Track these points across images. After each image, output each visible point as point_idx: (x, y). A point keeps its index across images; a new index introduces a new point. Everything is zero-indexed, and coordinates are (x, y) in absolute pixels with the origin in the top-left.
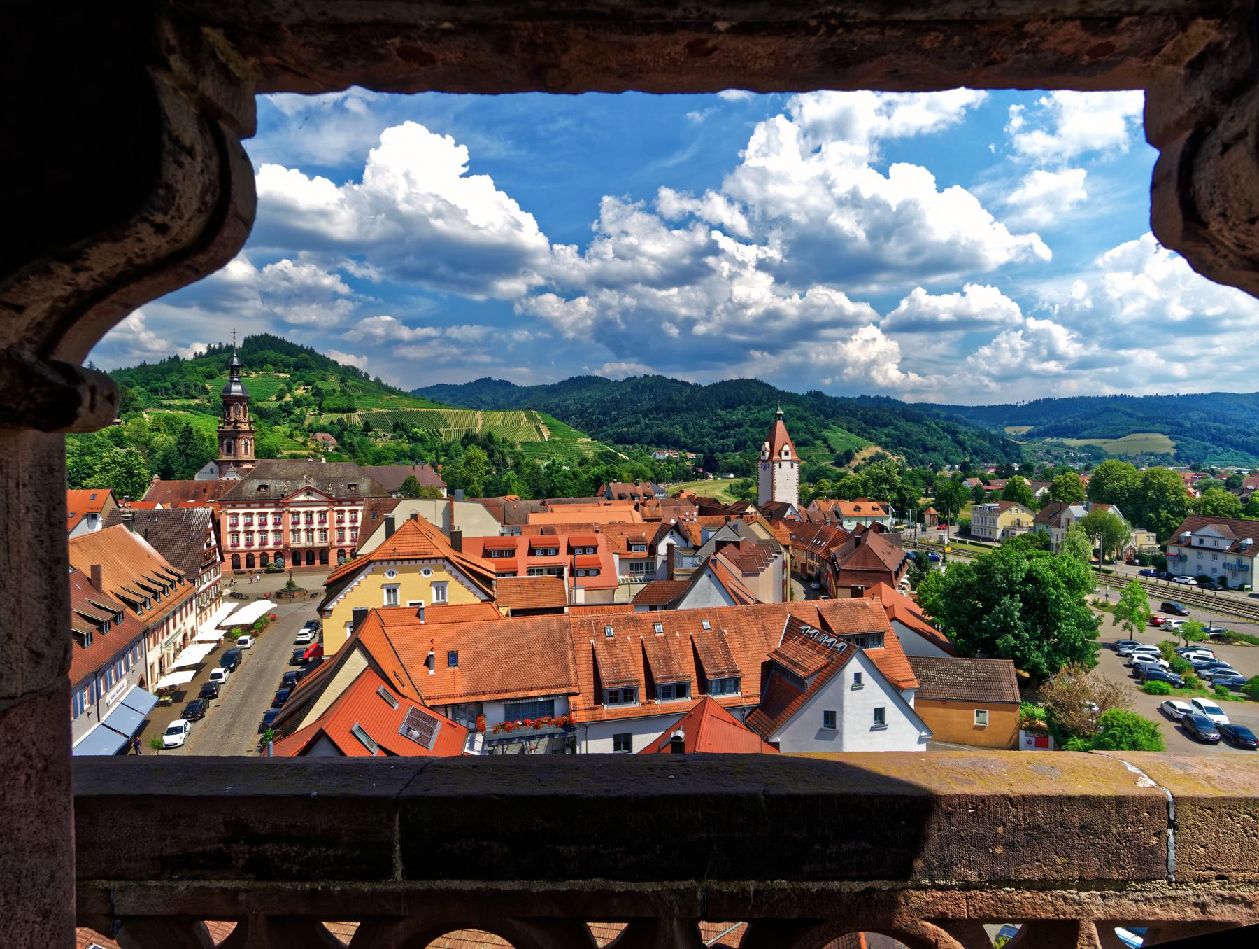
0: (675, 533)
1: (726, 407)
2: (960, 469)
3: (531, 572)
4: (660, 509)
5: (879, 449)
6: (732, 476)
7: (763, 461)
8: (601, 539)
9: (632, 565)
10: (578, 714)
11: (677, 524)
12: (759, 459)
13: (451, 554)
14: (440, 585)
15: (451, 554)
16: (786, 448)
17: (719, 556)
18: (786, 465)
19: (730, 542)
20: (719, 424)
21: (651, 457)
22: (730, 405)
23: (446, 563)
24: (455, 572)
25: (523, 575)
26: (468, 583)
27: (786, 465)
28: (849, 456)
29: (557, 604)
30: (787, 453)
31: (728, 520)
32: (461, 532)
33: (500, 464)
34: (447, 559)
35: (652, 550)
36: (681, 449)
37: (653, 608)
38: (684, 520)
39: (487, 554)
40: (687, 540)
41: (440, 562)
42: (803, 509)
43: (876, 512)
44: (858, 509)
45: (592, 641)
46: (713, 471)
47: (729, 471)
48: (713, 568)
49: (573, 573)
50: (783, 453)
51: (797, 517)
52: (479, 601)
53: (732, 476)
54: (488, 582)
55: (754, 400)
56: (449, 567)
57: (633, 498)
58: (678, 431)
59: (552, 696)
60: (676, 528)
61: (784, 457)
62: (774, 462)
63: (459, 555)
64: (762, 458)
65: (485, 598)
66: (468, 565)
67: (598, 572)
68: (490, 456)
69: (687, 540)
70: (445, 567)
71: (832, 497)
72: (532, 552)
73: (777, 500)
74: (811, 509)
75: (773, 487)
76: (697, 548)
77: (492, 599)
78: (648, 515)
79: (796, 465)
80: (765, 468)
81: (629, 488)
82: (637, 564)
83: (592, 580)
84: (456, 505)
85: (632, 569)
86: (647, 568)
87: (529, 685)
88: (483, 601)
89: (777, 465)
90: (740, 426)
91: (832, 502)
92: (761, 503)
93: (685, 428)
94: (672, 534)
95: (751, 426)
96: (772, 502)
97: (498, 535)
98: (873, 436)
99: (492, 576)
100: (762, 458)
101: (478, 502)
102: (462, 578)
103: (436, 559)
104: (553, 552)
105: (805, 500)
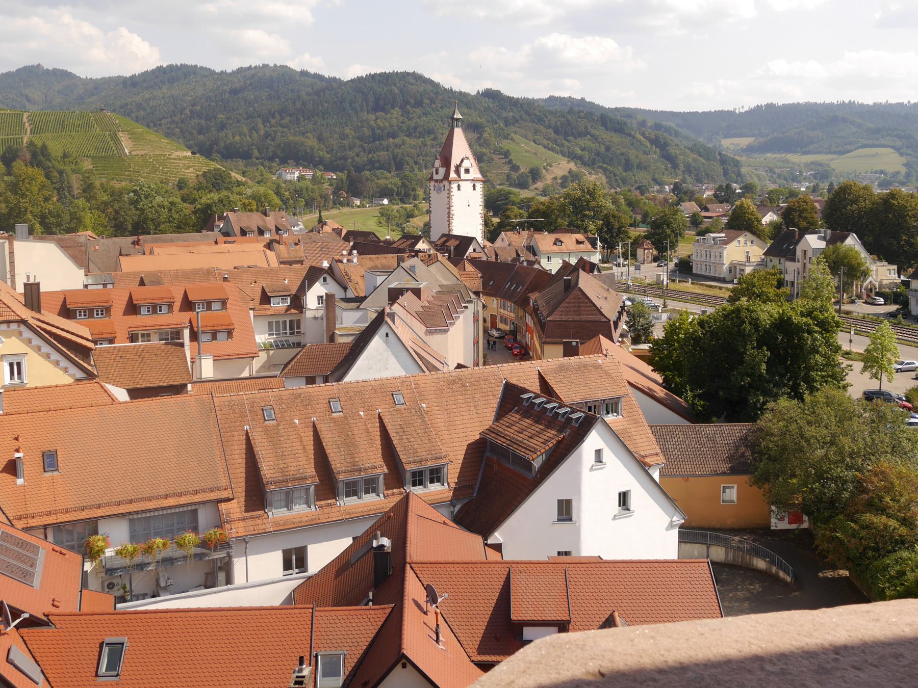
0: (329, 279)
1: (376, 108)
2: (673, 191)
3: (133, 338)
4: (301, 247)
5: (572, 166)
6: (386, 202)
7: (436, 181)
8: (230, 290)
9: (270, 324)
10: (234, 525)
11: (330, 268)
12: (431, 179)
13: (26, 314)
14: (15, 360)
15: (26, 314)
16: (466, 164)
17: (396, 308)
18: (466, 186)
19: (407, 290)
20: (367, 132)
21: (274, 178)
22: (380, 105)
23: (23, 328)
24: (37, 341)
25: (122, 344)
26: (55, 356)
27: (466, 186)
28: (535, 175)
29: (178, 382)
30: (467, 171)
31: (400, 260)
32: (38, 284)
33: (62, 190)
34: (23, 322)
35: (297, 302)
36: (315, 166)
37: (311, 381)
38: (341, 262)
39: (67, 312)
40: (345, 289)
41: (14, 326)
42: (488, 244)
43: (582, 246)
44: (557, 242)
45: (247, 427)
46: (357, 195)
47: (382, 195)
48: (391, 323)
49: (194, 336)
50: (462, 170)
51: (482, 255)
52: (71, 381)
53: (386, 202)
54: (85, 352)
55: (412, 101)
56: (27, 334)
57: (261, 232)
58: (311, 142)
59: (196, 504)
60: (331, 271)
61: (463, 176)
62: (450, 182)
63: (38, 316)
64: (435, 177)
65: (80, 374)
66: (54, 330)
67: (230, 334)
68: (47, 176)
69: (345, 289)
70: (21, 334)
71: (522, 226)
72: (132, 308)
73: (455, 233)
74: (498, 243)
75: (449, 216)
76: (360, 300)
77: (90, 376)
78: (285, 256)
79: (479, 186)
80: (439, 191)
81: (254, 220)
82: (277, 323)
83: (223, 344)
84: (17, 244)
85: (270, 329)
86: (291, 328)
87: (162, 492)
88: (79, 380)
89: (454, 186)
90: (394, 136)
91: (525, 233)
92: (435, 236)
93: (320, 139)
94: (325, 279)
95: (409, 135)
96: (449, 237)
97: (81, 287)
98: (565, 150)
99: (90, 345)
100: (435, 177)
101: (50, 241)
102: (46, 349)
103: (8, 322)
104: (165, 309)
105: (492, 234)
